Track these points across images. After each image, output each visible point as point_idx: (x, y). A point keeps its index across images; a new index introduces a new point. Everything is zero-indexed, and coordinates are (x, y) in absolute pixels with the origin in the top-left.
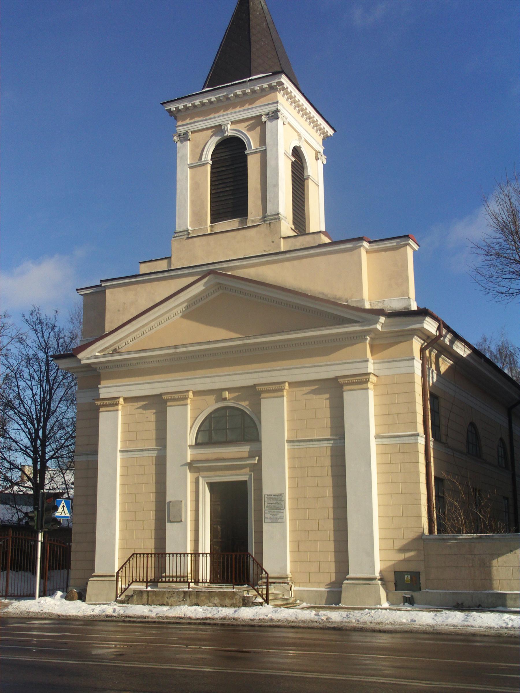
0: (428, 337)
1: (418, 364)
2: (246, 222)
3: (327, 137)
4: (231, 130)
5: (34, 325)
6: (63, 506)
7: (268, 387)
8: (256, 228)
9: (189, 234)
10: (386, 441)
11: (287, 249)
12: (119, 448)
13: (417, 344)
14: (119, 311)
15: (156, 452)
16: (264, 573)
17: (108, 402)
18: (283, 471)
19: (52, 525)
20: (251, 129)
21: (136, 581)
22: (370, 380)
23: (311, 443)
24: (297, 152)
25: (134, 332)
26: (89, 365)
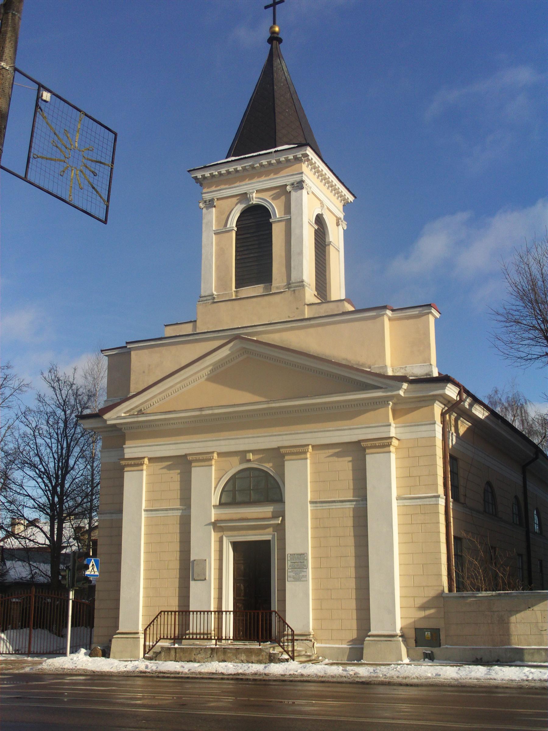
0: (449, 402)
1: (439, 428)
2: (271, 289)
3: (348, 203)
4: (256, 198)
5: (52, 383)
6: (93, 565)
7: (293, 450)
8: (281, 295)
9: (214, 298)
11: (311, 316)
12: (144, 507)
13: (438, 408)
14: (144, 372)
15: (181, 511)
16: (290, 630)
17: (132, 462)
18: (305, 530)
19: (83, 584)
20: (275, 198)
21: (164, 638)
22: (392, 443)
23: (334, 504)
24: (319, 220)
25: (160, 393)
26: (114, 425)
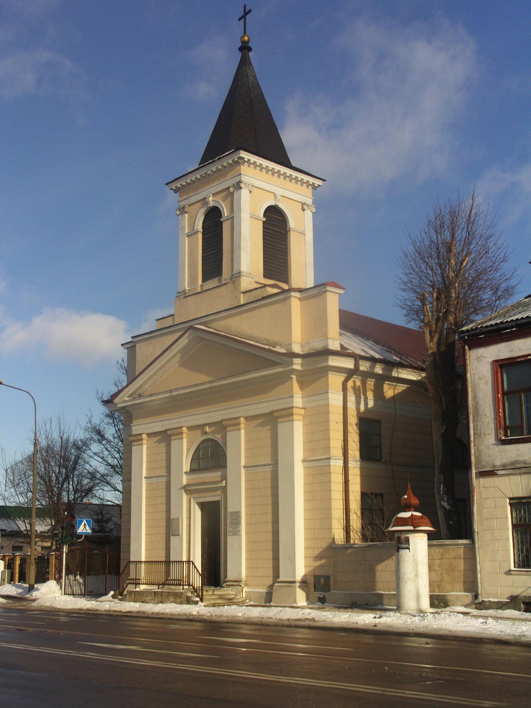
6: (85, 525)
8: (226, 286)
10: (310, 464)
14: (144, 361)
15: (166, 478)
22: (294, 412)
23: (259, 468)
26: (123, 408)
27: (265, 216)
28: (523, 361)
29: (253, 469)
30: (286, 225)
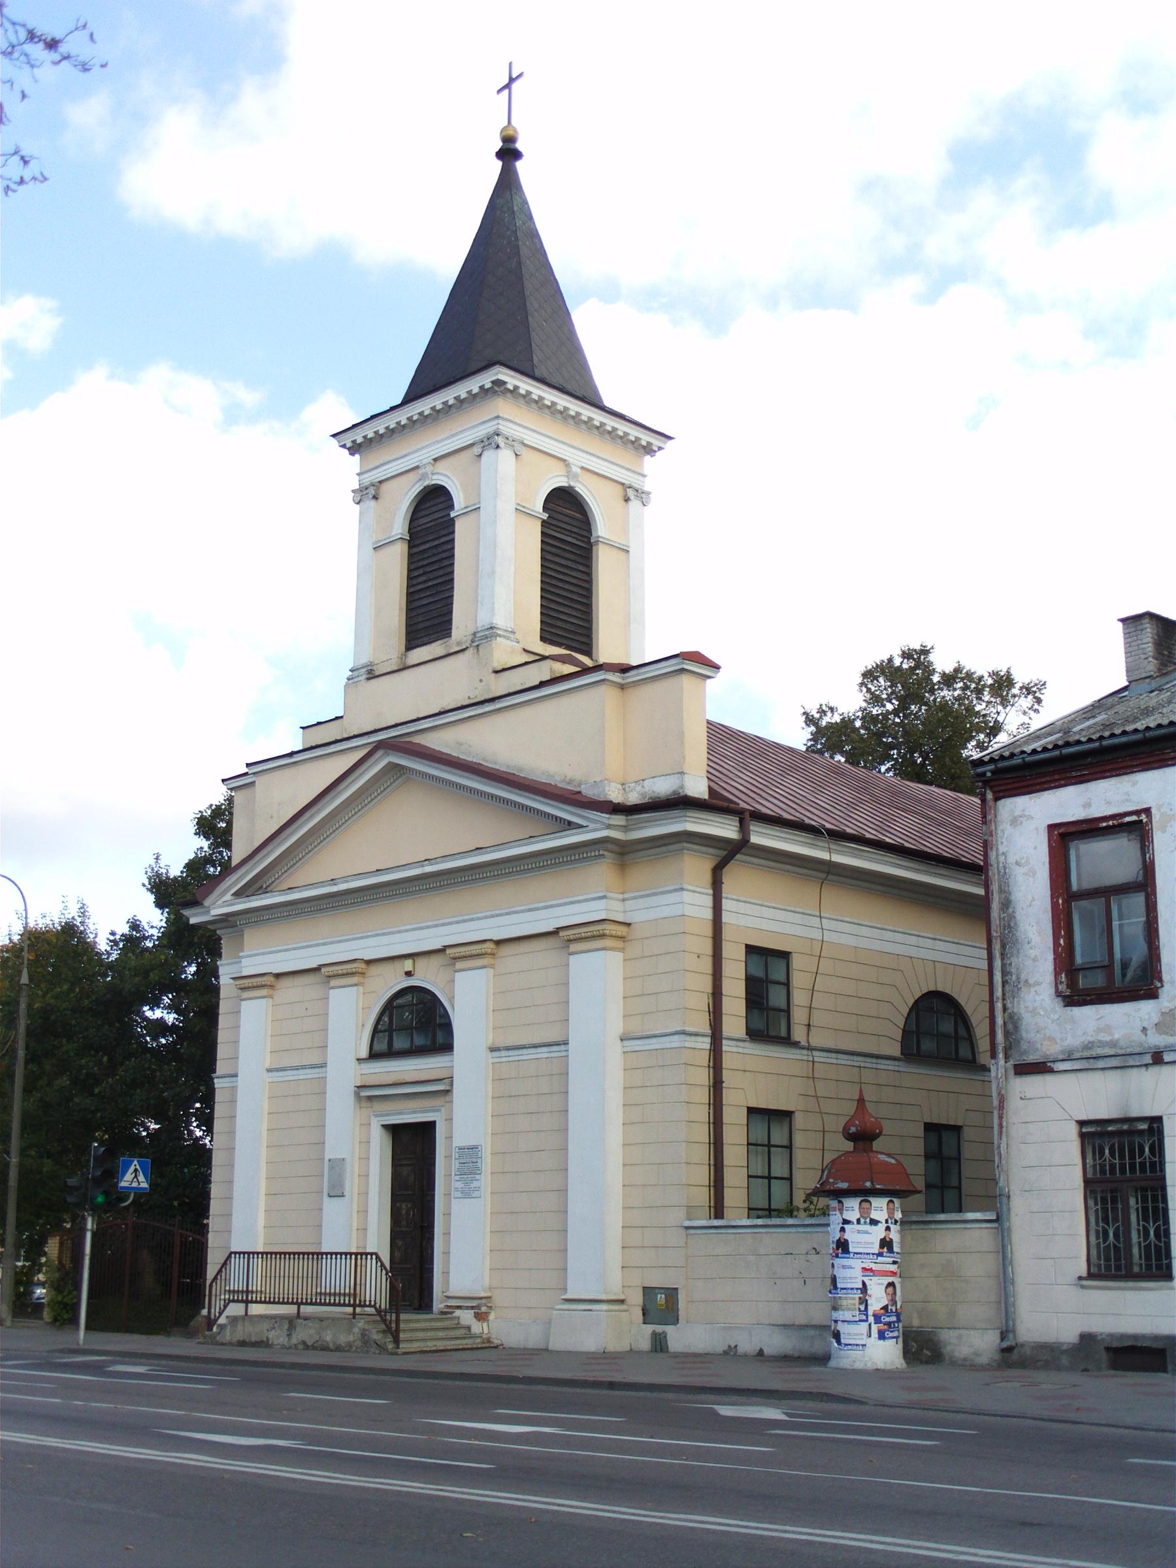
6: (136, 1170)
23: (525, 1051)
27: (545, 509)
28: (1114, 826)
29: (511, 1053)
30: (590, 531)
